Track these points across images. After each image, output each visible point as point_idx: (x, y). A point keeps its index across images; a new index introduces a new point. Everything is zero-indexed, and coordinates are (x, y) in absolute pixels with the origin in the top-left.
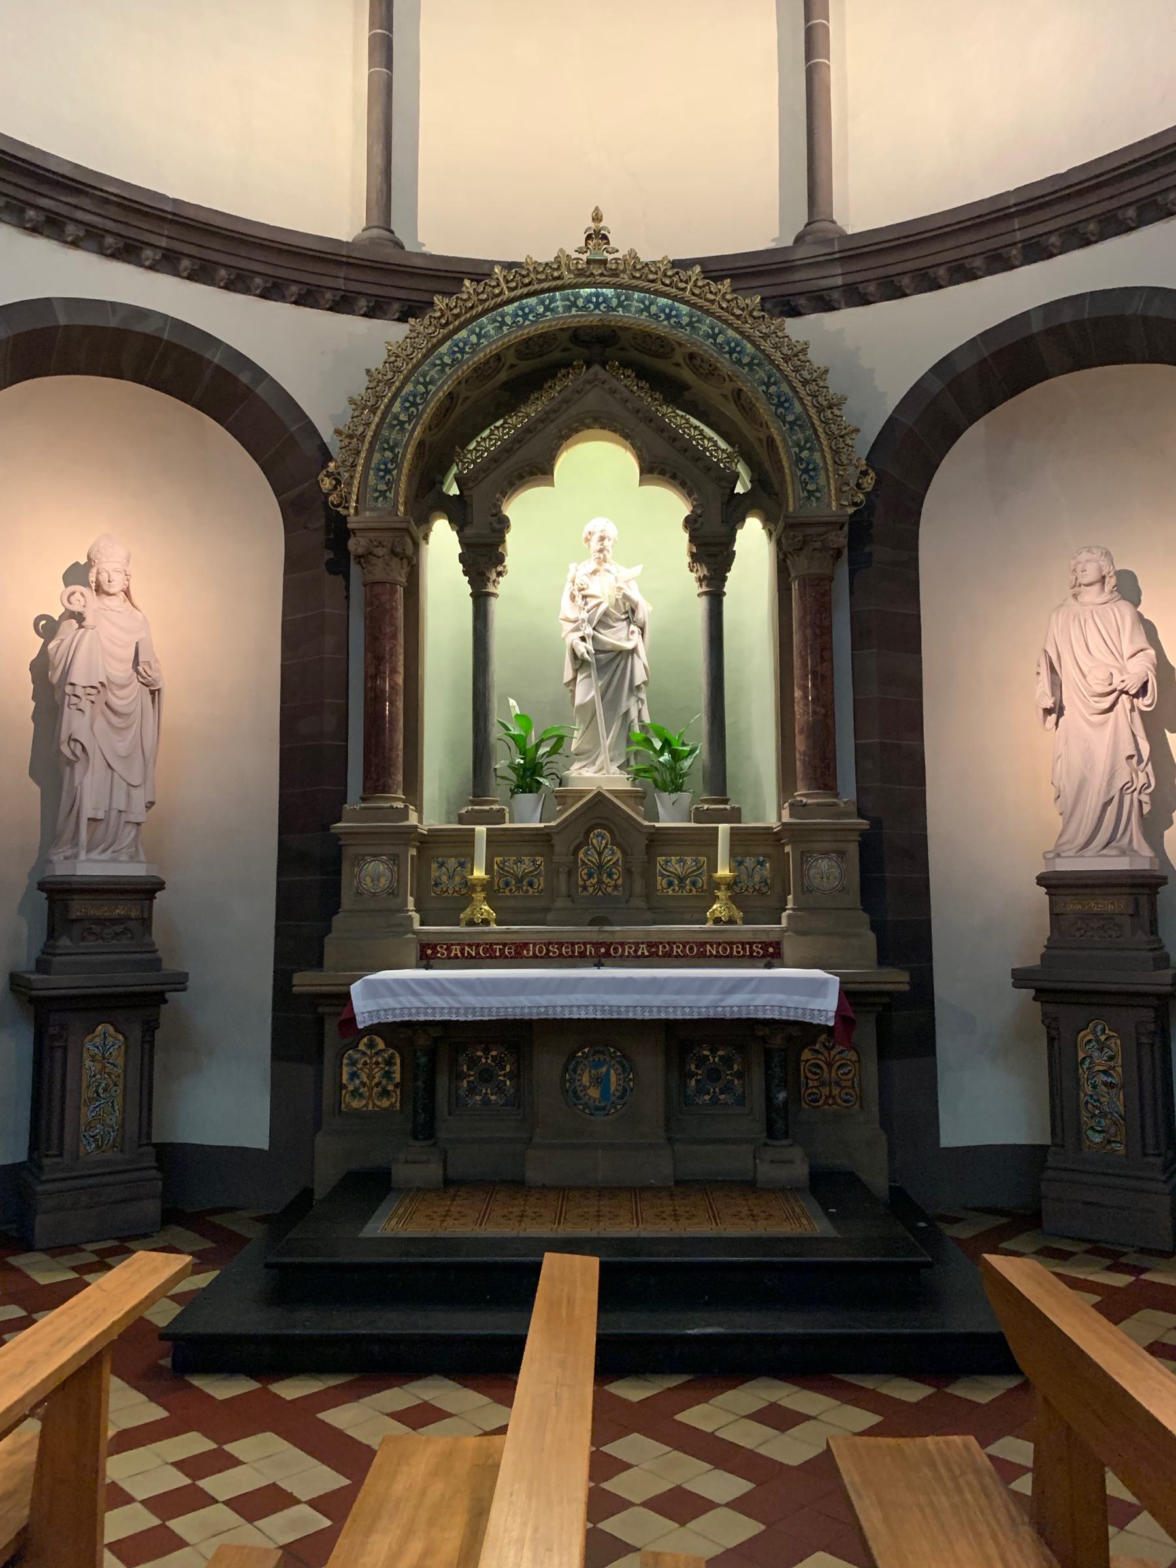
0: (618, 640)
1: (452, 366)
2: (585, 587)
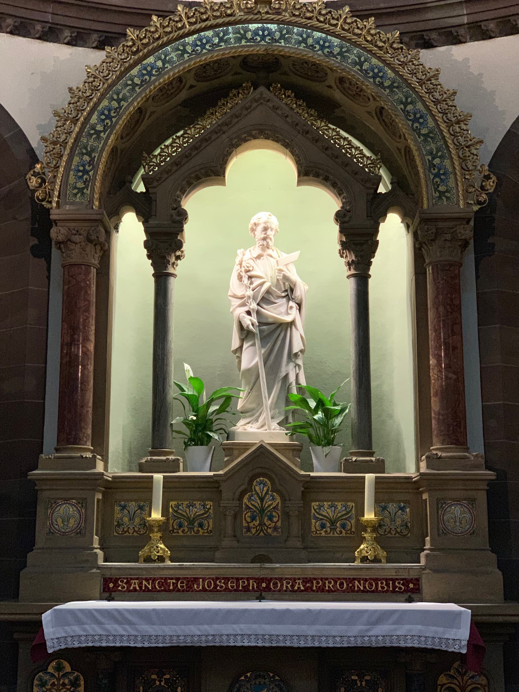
0: (278, 314)
1: (141, 86)
2: (251, 269)
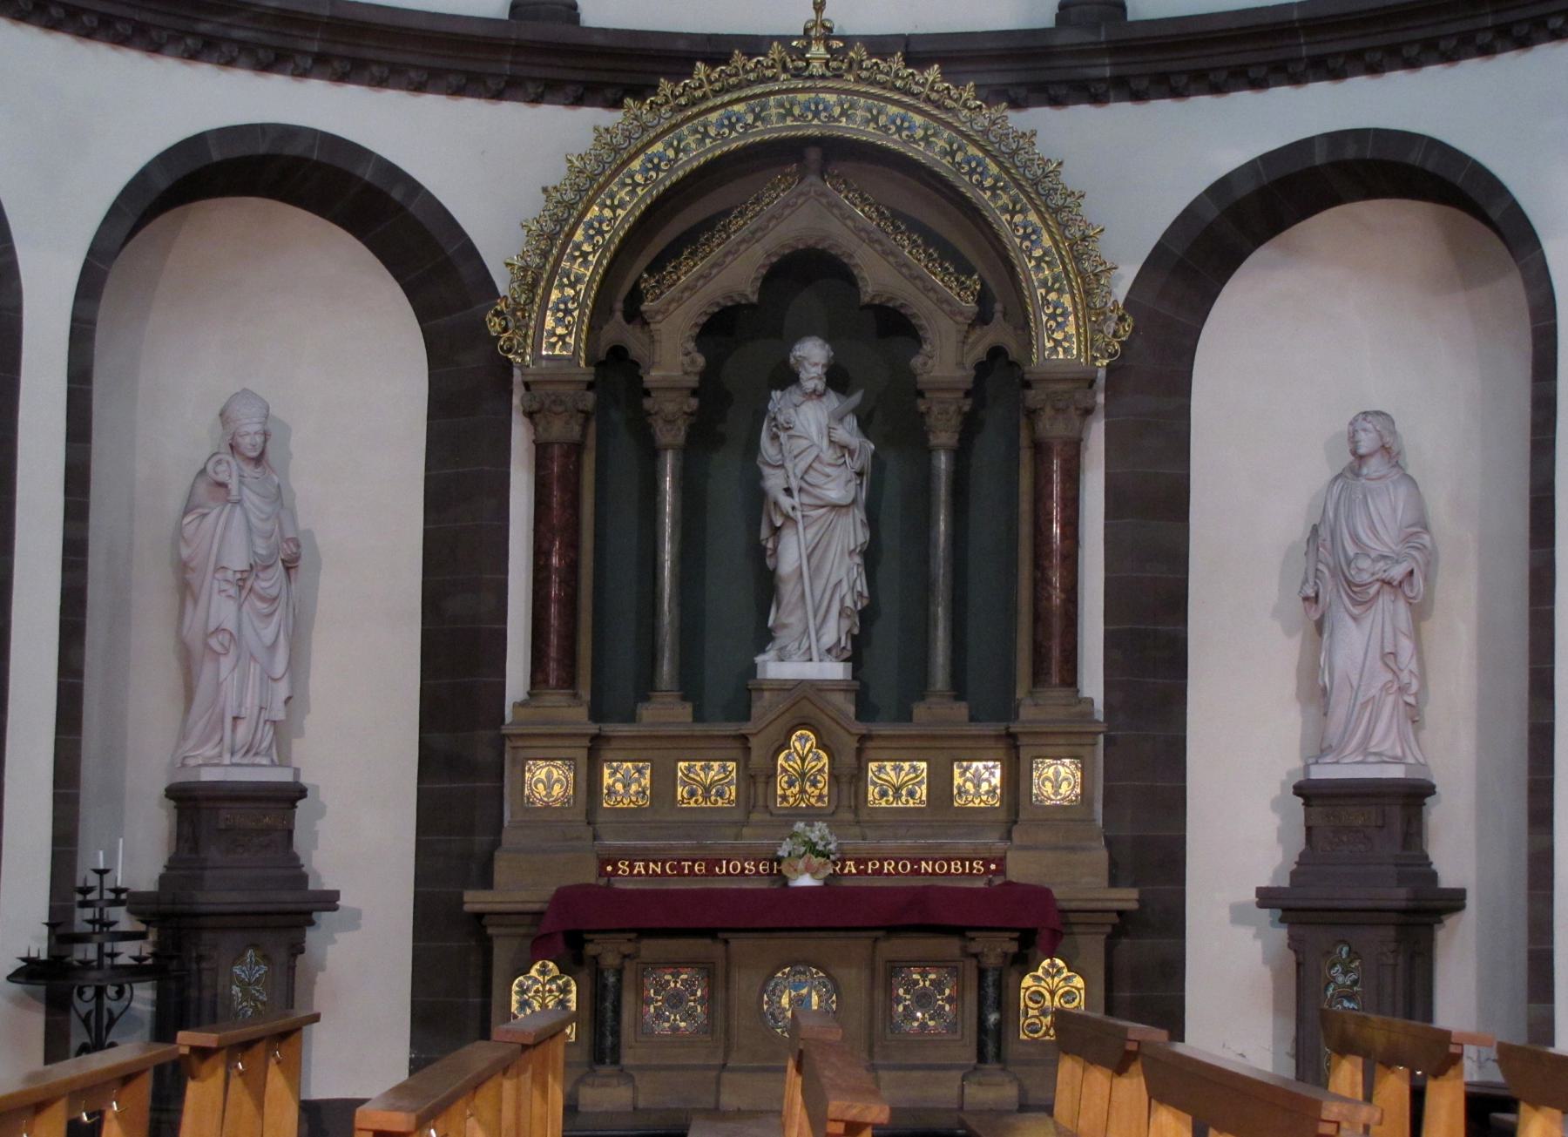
1: (645, 185)
